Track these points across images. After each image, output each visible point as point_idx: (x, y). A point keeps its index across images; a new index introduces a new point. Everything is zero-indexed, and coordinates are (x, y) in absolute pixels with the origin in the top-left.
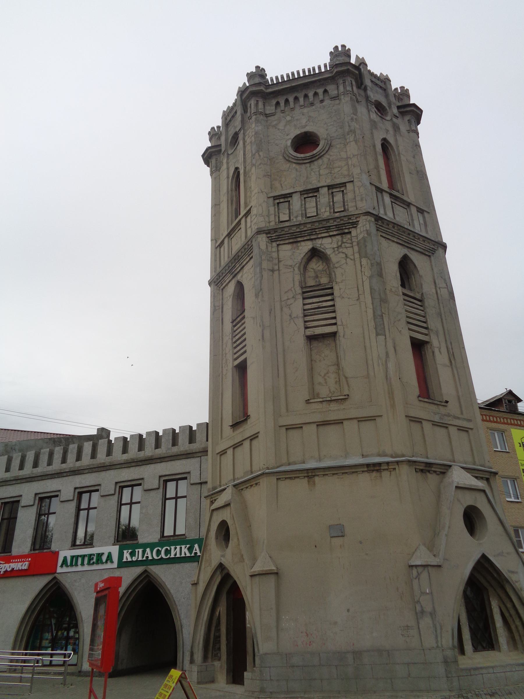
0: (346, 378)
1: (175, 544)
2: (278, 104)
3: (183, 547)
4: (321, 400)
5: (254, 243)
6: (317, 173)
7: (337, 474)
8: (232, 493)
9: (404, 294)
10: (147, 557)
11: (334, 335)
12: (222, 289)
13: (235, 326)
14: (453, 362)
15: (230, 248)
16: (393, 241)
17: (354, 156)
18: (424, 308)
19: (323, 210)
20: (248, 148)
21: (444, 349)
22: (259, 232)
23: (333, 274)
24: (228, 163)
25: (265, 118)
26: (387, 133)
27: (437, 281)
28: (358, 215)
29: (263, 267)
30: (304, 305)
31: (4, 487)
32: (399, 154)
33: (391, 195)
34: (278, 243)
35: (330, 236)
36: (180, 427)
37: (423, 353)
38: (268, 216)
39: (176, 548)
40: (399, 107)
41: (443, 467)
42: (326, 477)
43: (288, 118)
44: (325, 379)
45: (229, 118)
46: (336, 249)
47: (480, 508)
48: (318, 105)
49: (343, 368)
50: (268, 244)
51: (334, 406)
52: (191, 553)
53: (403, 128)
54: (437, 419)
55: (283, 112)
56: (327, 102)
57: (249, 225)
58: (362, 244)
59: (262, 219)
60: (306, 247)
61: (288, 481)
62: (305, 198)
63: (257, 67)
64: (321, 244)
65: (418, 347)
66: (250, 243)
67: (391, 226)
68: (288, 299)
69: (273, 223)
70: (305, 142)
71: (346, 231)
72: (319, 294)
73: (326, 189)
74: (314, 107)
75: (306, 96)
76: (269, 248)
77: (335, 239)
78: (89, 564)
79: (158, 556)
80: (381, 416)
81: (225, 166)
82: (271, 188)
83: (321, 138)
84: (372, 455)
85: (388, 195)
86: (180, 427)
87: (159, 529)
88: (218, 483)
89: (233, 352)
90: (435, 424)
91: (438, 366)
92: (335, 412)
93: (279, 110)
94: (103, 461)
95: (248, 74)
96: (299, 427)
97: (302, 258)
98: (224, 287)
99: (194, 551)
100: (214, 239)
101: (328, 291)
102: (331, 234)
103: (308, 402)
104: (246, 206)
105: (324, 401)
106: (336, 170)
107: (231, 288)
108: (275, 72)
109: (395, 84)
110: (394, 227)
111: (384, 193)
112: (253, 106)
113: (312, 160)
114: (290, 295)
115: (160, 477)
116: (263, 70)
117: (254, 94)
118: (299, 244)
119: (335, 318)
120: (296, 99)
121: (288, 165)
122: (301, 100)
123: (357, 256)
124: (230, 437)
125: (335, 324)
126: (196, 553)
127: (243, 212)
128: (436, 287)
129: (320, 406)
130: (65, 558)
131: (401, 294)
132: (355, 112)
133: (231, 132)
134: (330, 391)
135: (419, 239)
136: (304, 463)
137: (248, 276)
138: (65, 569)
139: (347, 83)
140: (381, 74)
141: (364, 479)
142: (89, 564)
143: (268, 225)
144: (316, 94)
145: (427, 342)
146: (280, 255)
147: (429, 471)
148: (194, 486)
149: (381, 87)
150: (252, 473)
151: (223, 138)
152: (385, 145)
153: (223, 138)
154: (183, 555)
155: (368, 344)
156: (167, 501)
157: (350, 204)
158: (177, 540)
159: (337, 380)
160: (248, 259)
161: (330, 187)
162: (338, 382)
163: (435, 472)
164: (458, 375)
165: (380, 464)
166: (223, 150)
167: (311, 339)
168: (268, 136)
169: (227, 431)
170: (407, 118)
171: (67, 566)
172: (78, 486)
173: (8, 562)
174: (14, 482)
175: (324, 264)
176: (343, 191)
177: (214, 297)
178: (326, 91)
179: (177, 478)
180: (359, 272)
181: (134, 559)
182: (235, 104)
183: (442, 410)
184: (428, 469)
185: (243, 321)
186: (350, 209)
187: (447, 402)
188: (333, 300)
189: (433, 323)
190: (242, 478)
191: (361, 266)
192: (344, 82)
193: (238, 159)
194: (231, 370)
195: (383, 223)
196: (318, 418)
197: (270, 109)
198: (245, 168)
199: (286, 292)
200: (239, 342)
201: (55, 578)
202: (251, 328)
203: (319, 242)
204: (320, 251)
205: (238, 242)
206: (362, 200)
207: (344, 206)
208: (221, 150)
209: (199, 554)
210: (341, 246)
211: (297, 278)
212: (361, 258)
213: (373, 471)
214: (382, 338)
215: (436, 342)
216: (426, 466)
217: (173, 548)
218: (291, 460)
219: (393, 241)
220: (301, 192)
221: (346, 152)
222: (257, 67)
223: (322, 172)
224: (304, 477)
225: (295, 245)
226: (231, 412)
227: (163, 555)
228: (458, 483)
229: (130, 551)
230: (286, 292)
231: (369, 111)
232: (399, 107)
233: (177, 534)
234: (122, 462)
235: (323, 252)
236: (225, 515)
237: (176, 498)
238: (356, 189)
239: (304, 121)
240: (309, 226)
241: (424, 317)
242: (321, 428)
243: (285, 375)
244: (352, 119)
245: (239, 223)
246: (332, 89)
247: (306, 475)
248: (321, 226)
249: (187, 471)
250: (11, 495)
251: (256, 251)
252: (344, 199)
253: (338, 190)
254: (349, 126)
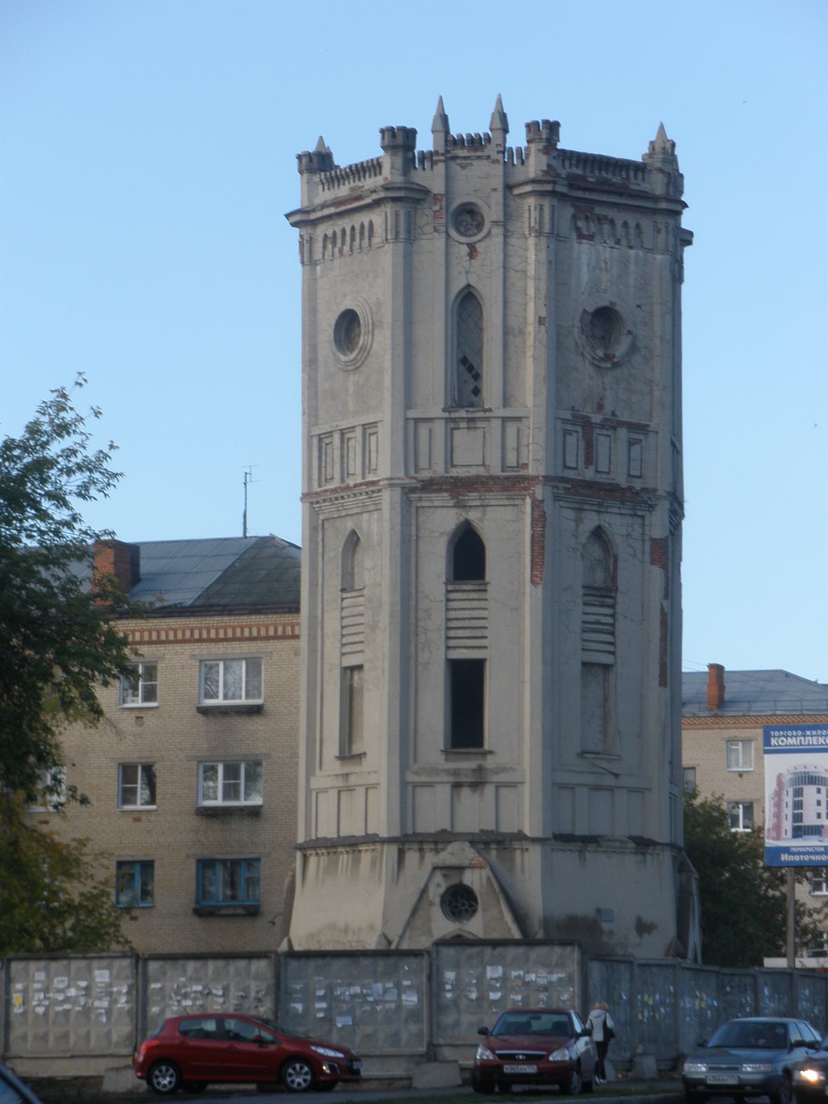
11: (607, 667)
35: (620, 514)
60: (591, 520)
144: (625, 224)
167: (584, 664)
203: (606, 517)
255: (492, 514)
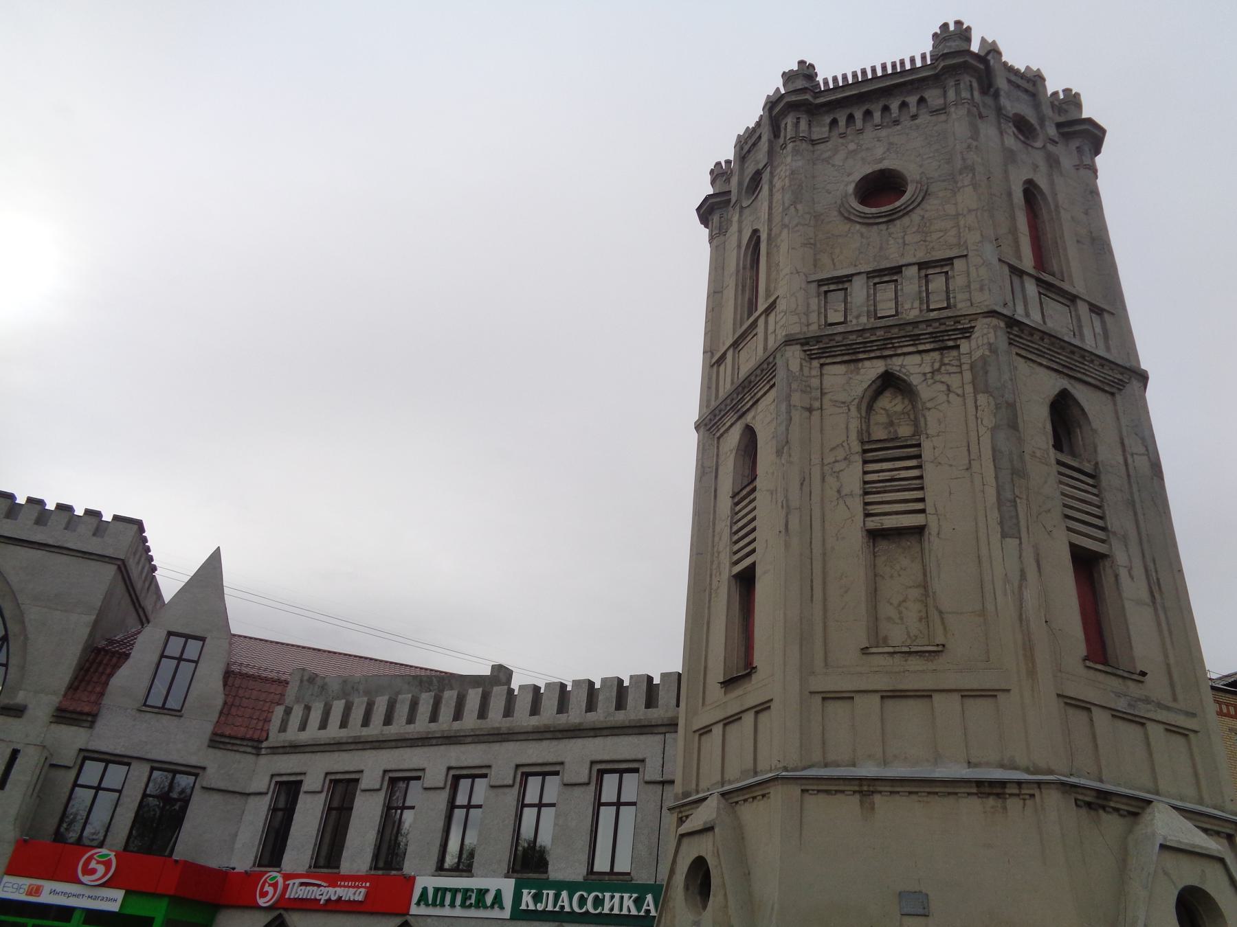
0: (941, 612)
1: (613, 889)
2: (834, 122)
3: (626, 896)
4: (891, 650)
5: (779, 362)
6: (900, 241)
7: (917, 793)
8: (718, 808)
9: (1059, 463)
10: (562, 907)
11: (920, 530)
12: (719, 438)
13: (737, 504)
14: (1157, 596)
15: (736, 367)
16: (1041, 364)
17: (970, 211)
18: (1100, 491)
19: (907, 306)
20: (777, 196)
21: (1139, 571)
22: (789, 341)
23: (922, 420)
24: (740, 222)
25: (810, 147)
26: (1035, 170)
27: (1126, 442)
28: (974, 317)
29: (792, 403)
30: (865, 473)
31: (336, 754)
32: (1057, 206)
33: (1040, 282)
34: (822, 361)
35: (919, 352)
36: (631, 677)
37: (1095, 575)
38: (807, 314)
39: (612, 897)
40: (1059, 125)
41: (1134, 803)
42: (897, 797)
43: (852, 146)
44: (900, 613)
45: (746, 148)
46: (929, 376)
47: (1212, 894)
48: (906, 122)
49: (934, 593)
50: (804, 364)
51: (915, 664)
52: (639, 910)
53: (1067, 162)
54: (1121, 705)
55: (843, 136)
56: (924, 118)
57: (771, 328)
58: (979, 369)
59: (795, 319)
60: (872, 370)
61: (822, 796)
62: (875, 284)
63: (801, 63)
64: (902, 366)
65: (1087, 565)
66: (771, 359)
67: (1036, 337)
68: (836, 461)
69: (814, 327)
70: (881, 188)
71: (951, 343)
72: (892, 455)
73: (916, 268)
74: (899, 127)
75: (886, 109)
76: (806, 370)
77: (927, 358)
78: (463, 905)
79: (581, 907)
80: (1008, 691)
81: (734, 227)
82: (815, 266)
83: (909, 179)
84: (988, 764)
85: (1033, 281)
86: (631, 677)
87: (584, 857)
88: (694, 786)
89: (731, 549)
90: (1117, 715)
91: (1127, 604)
92: (917, 675)
93: (835, 133)
94: (497, 725)
95: (784, 74)
96: (846, 697)
97: (866, 390)
98: (722, 435)
99: (645, 907)
100: (708, 351)
101: (911, 450)
102: (921, 348)
103: (865, 651)
104: (768, 296)
105: (895, 653)
106: (935, 236)
107: (734, 437)
108: (833, 67)
109: (1054, 85)
110: (1042, 339)
111: (1025, 277)
112: (789, 127)
113: (891, 218)
114: (840, 454)
115: (592, 763)
116: (812, 66)
117: (793, 107)
118: (860, 365)
119: (922, 500)
120: (868, 114)
121: (848, 226)
122: (877, 116)
123: (969, 389)
124: (718, 703)
125: (923, 511)
126: (648, 911)
127: (762, 306)
128: (1124, 451)
129: (887, 661)
130: (425, 890)
131: (1053, 462)
132: (975, 135)
133: (750, 170)
134: (908, 634)
135: (1092, 361)
136: (854, 765)
137: (765, 417)
138: (423, 910)
139: (962, 85)
140: (1028, 68)
141: (971, 808)
142: (463, 905)
143: (805, 329)
144: (904, 105)
145: (1104, 556)
146: (825, 382)
147: (1104, 808)
148: (651, 787)
149: (1026, 91)
150: (756, 773)
151: (734, 181)
152: (1031, 193)
153: (734, 181)
154: (625, 912)
155: (984, 551)
156: (602, 809)
157: (960, 297)
158: (616, 881)
159: (924, 614)
160: (767, 387)
161: (922, 266)
162: (925, 619)
163: (1117, 810)
164: (1168, 624)
165: (1003, 784)
166: (733, 200)
167: (875, 535)
168: (814, 177)
169: (715, 692)
170: (1074, 144)
171: (427, 905)
172: (453, 764)
173: (334, 885)
174: (352, 747)
175: (906, 402)
176: (947, 273)
177: (703, 450)
178: (922, 100)
179: (623, 769)
180: (971, 418)
181: (540, 907)
182: (758, 124)
183: (1134, 689)
184: (1100, 802)
185: (752, 497)
186: (959, 306)
187: (1143, 674)
188: (919, 467)
189: (1118, 519)
190: (737, 780)
191: (977, 407)
192: (957, 85)
193: (758, 216)
194: (726, 583)
195: (1022, 331)
196: (884, 683)
197: (820, 131)
198: (770, 230)
199: (832, 449)
200: (744, 533)
201: (406, 923)
202: (766, 509)
203: (897, 361)
204: (899, 378)
205: (749, 359)
206: (981, 289)
207: (948, 299)
208: (729, 201)
209: (653, 913)
210: (939, 370)
211: (854, 425)
212: (976, 392)
213: (989, 794)
214: (1012, 543)
215: (1121, 556)
216: (1098, 797)
217: (608, 895)
218: (831, 757)
219: (1041, 364)
220: (868, 273)
221: (956, 204)
222: (801, 63)
223: (908, 239)
224: (855, 792)
225: (852, 366)
226: (722, 658)
227: (589, 906)
228: (1165, 838)
229: (533, 891)
230: (832, 449)
231: (1001, 133)
232: (1059, 125)
233: (616, 870)
234: (529, 730)
235: (904, 381)
236: (703, 847)
237: (618, 804)
238: (973, 270)
239: (879, 151)
240: (880, 333)
241: (1099, 507)
242: (890, 704)
243: (825, 600)
244: (969, 147)
245: (755, 323)
246: (933, 96)
247: (857, 788)
248: (902, 333)
249: (640, 757)
250: (347, 769)
251: (781, 374)
252: (947, 288)
253: (938, 270)
254: (964, 159)
255: (762, 405)
